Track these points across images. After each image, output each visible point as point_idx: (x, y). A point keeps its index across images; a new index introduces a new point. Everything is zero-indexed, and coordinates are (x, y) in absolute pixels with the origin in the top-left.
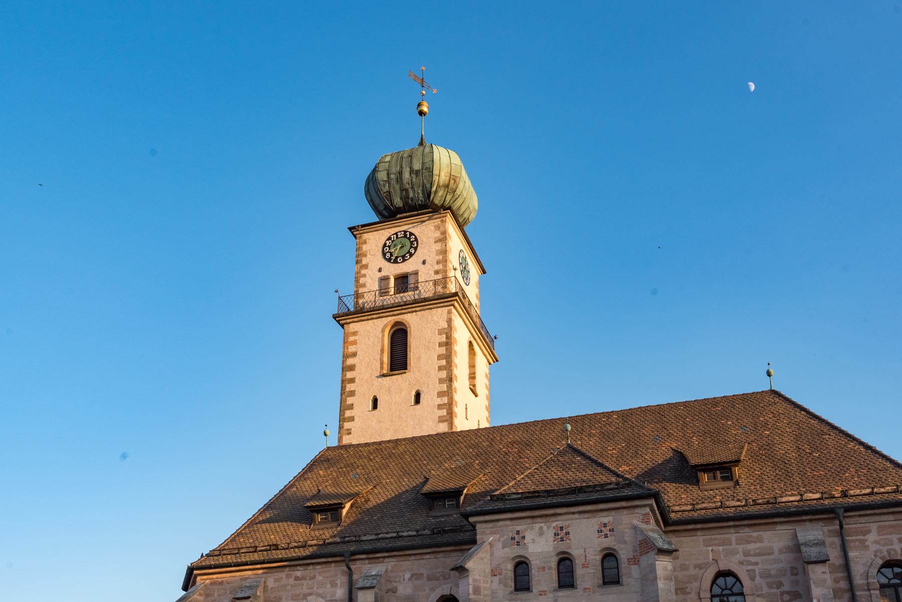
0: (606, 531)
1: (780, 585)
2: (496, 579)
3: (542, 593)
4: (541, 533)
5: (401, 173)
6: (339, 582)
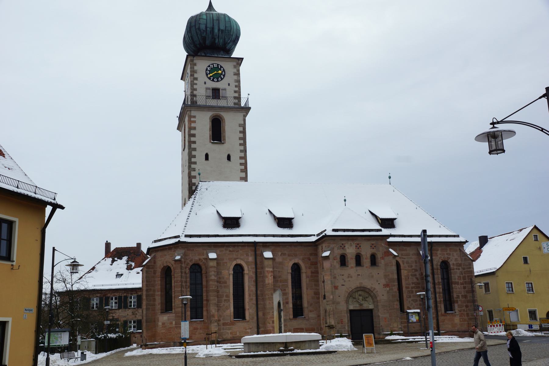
0: (373, 246)
1: (412, 266)
2: (335, 261)
3: (352, 267)
4: (351, 246)
5: (213, 28)
6: (250, 254)
